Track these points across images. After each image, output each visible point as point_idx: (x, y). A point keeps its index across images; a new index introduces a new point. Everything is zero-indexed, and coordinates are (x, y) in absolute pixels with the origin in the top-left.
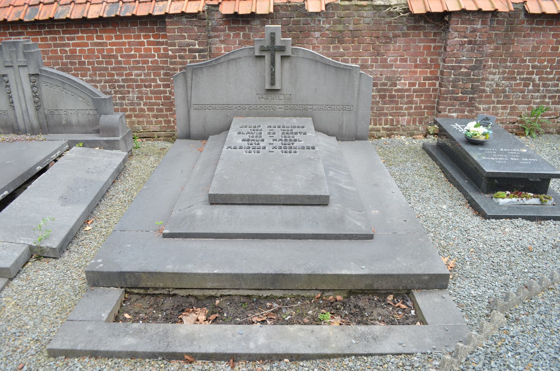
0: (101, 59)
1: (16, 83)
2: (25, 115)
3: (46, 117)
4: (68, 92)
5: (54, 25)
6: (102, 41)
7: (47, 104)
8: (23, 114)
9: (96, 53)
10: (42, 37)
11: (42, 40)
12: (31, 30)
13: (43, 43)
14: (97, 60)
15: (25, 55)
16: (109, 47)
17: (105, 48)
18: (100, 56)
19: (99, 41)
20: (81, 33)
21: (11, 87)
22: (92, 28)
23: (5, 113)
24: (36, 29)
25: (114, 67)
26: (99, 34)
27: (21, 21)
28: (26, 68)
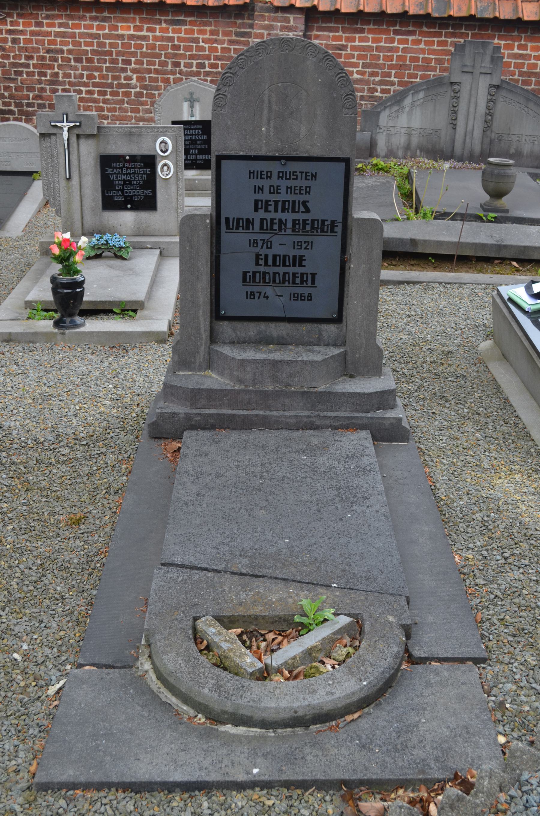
0: (516, 77)
1: (470, 95)
2: (468, 137)
3: (491, 142)
4: (531, 112)
5: (462, 25)
6: (525, 52)
7: (498, 125)
8: (465, 136)
9: (512, 69)
10: (440, 39)
11: (440, 43)
12: (426, 30)
13: (440, 48)
14: (511, 77)
15: (493, 59)
16: (533, 61)
17: (526, 62)
18: (517, 73)
19: (521, 52)
20: (498, 39)
21: (461, 100)
22: (516, 33)
23: (436, 133)
24: (435, 28)
25: (533, 89)
26: (523, 42)
27: (428, 16)
28: (489, 76)
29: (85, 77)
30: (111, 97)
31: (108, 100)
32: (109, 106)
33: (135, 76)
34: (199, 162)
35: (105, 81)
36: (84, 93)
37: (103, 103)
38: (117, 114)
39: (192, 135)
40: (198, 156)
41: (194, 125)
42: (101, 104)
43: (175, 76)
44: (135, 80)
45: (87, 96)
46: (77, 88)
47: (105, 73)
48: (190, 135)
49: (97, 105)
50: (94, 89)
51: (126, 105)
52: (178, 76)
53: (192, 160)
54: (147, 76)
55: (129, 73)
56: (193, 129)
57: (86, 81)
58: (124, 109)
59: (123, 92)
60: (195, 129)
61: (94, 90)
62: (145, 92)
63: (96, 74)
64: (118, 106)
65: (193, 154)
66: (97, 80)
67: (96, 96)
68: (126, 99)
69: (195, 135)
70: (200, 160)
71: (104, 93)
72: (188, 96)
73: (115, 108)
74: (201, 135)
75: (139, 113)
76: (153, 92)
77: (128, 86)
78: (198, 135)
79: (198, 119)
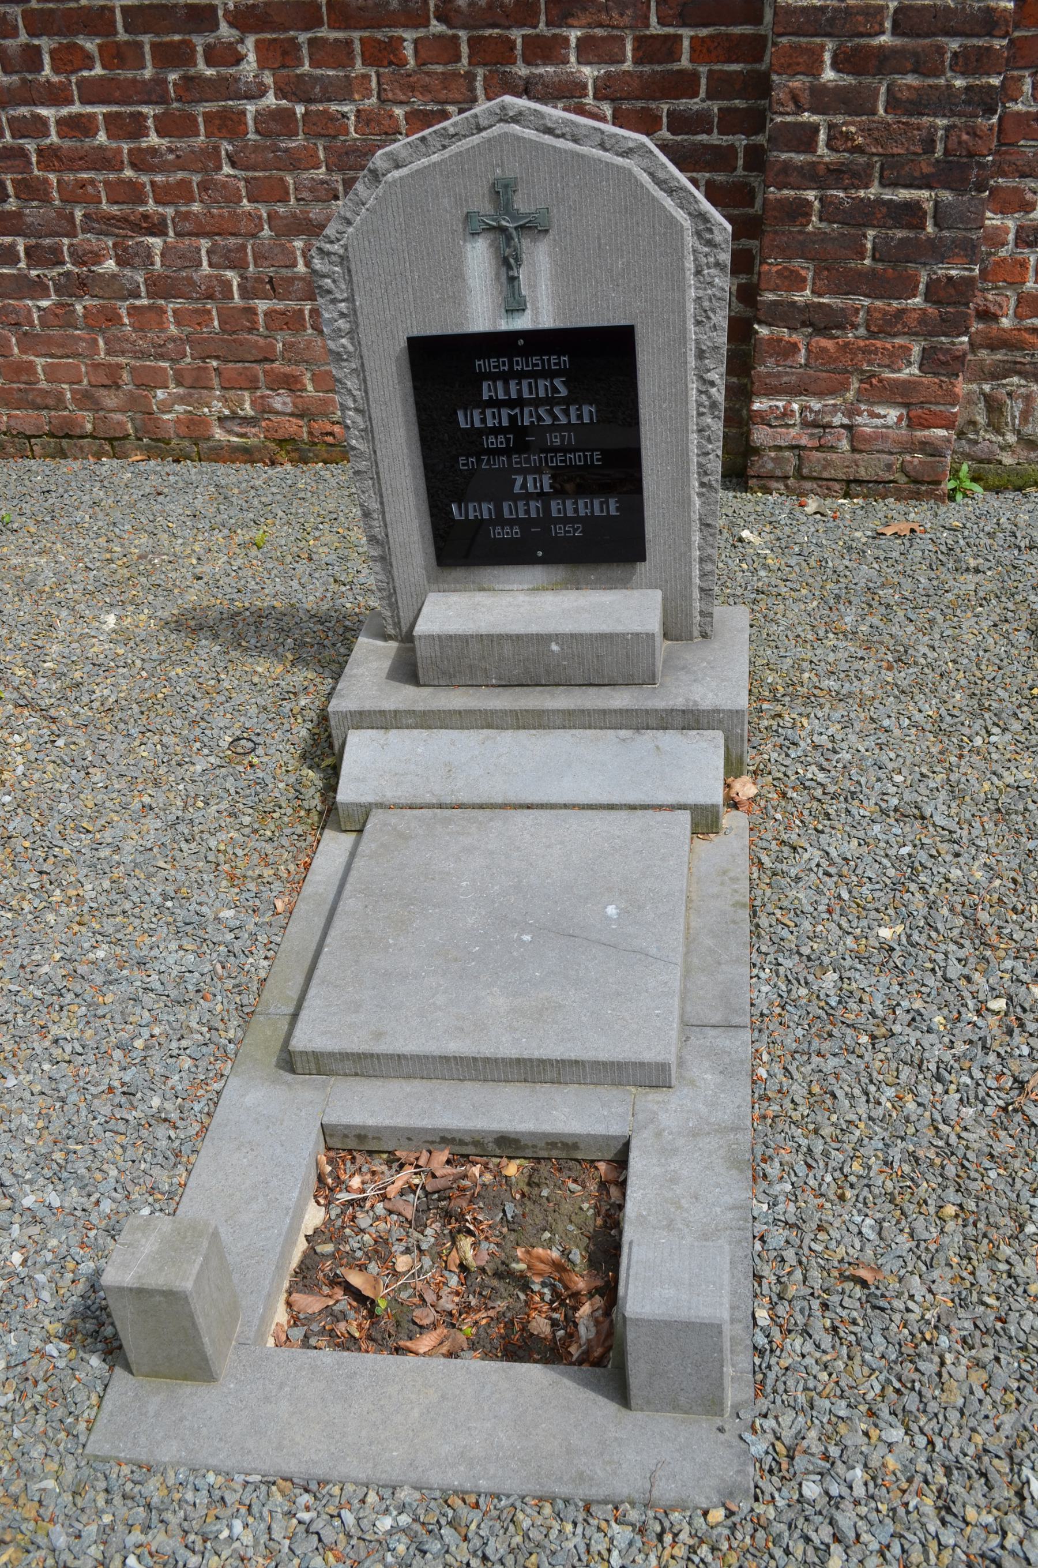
29: (46, 59)
30: (165, 142)
31: (153, 151)
32: (159, 178)
33: (250, 41)
34: (559, 531)
35: (130, 74)
36: (53, 130)
37: (134, 166)
38: (196, 207)
39: (520, 402)
40: (554, 505)
41: (526, 352)
42: (128, 173)
43: (421, 33)
44: (252, 57)
45: (67, 144)
46: (23, 111)
47: (122, 36)
48: (510, 403)
49: (112, 176)
50: (89, 109)
51: (227, 169)
52: (437, 27)
53: (525, 524)
54: (303, 37)
55: (225, 31)
56: (521, 375)
57: (55, 79)
58: (224, 185)
59: (208, 117)
60: (535, 375)
61: (92, 117)
62: (300, 109)
63: (90, 45)
64: (196, 178)
65: (528, 497)
66: (98, 71)
67: (102, 137)
68: (226, 147)
69: (537, 402)
70: (565, 520)
71: (135, 128)
72: (484, 206)
73: (184, 184)
74: (567, 402)
75: (284, 199)
76: (334, 107)
77: (226, 88)
78: (550, 402)
79: (547, 320)
